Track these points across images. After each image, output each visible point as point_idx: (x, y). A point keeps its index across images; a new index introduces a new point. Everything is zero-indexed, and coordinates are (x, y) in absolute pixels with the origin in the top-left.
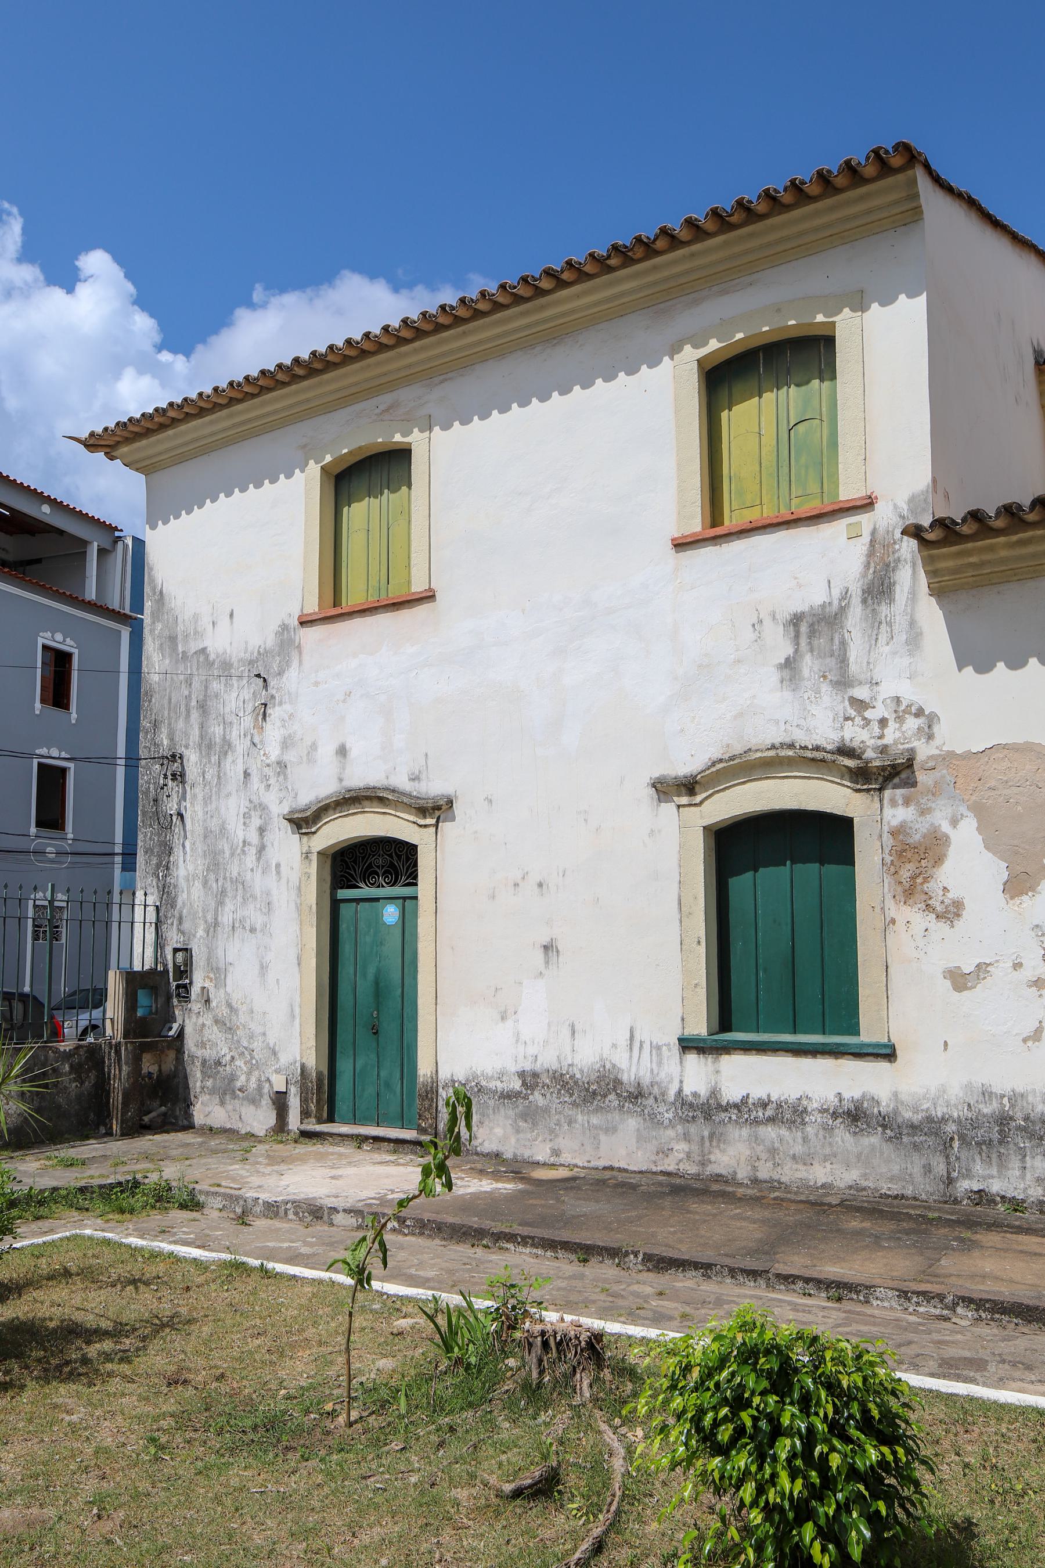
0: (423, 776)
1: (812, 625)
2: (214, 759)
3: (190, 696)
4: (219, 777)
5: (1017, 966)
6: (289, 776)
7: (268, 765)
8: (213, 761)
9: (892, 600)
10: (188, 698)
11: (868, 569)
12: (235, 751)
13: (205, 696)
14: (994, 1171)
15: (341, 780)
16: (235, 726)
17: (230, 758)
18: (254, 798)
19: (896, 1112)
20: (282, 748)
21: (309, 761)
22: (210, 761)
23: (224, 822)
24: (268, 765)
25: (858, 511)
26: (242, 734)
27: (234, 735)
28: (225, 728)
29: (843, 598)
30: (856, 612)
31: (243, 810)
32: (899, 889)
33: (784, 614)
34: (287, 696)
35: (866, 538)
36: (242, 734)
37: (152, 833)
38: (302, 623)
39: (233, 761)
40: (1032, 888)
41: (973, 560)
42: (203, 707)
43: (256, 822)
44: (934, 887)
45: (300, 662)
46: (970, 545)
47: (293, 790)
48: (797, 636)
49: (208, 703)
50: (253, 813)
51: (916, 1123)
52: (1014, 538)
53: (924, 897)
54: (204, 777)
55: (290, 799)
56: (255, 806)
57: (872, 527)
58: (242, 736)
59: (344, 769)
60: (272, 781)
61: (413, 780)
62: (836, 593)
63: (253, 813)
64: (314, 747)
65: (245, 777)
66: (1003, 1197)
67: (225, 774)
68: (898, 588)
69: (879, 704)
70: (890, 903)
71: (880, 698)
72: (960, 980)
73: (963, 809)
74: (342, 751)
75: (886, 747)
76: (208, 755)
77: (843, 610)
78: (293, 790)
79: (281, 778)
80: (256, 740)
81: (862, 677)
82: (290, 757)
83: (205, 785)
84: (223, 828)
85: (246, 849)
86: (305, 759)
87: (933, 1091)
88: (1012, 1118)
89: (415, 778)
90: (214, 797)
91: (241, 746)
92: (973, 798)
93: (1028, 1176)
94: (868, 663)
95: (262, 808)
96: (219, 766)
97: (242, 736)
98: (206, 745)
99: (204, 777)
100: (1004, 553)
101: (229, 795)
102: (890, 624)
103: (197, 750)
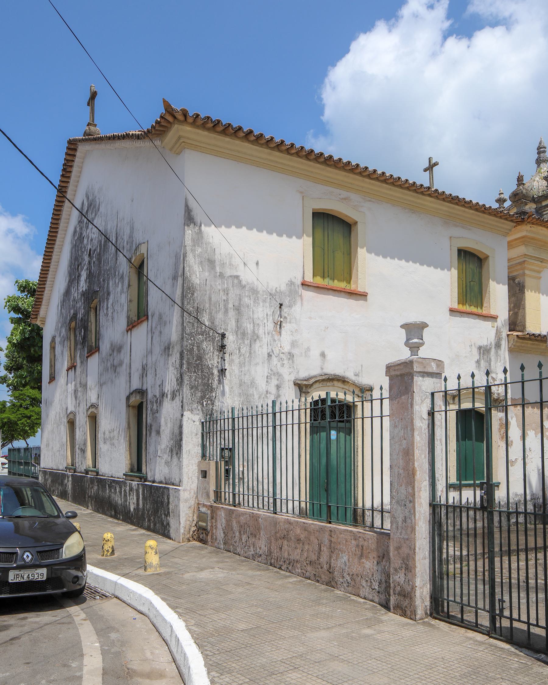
0: (360, 375)
1: (483, 351)
2: (247, 342)
3: (227, 300)
4: (250, 353)
6: (295, 361)
7: (283, 353)
8: (246, 343)
10: (226, 301)
12: (262, 341)
13: (239, 304)
15: (322, 369)
16: (261, 328)
17: (258, 344)
18: (274, 369)
20: (291, 346)
21: (306, 356)
22: (244, 343)
23: (253, 379)
24: (283, 353)
26: (266, 332)
27: (261, 332)
28: (254, 326)
29: (490, 345)
30: (493, 351)
31: (266, 374)
32: (501, 436)
33: (477, 345)
34: (294, 320)
35: (495, 328)
36: (266, 332)
37: (196, 377)
38: (302, 284)
39: (261, 346)
42: (238, 309)
43: (274, 382)
45: (302, 304)
47: (297, 369)
48: (480, 353)
49: (242, 309)
50: (273, 377)
54: (239, 351)
55: (295, 373)
56: (274, 374)
58: (266, 334)
59: (324, 364)
60: (285, 362)
61: (356, 375)
62: (489, 342)
63: (273, 377)
64: (308, 349)
65: (268, 357)
67: (254, 352)
68: (502, 346)
69: (498, 380)
70: (499, 440)
71: (498, 378)
73: (513, 415)
74: (323, 355)
75: (499, 393)
76: (243, 339)
77: (490, 348)
78: (297, 369)
79: (291, 361)
80: (276, 337)
82: (295, 351)
83: (240, 356)
84: (253, 383)
85: (268, 395)
86: (304, 354)
89: (356, 375)
90: (246, 363)
91: (266, 339)
95: (279, 375)
96: (251, 347)
97: (266, 334)
98: (241, 333)
99: (239, 351)
101: (257, 364)
102: (500, 356)
103: (234, 334)
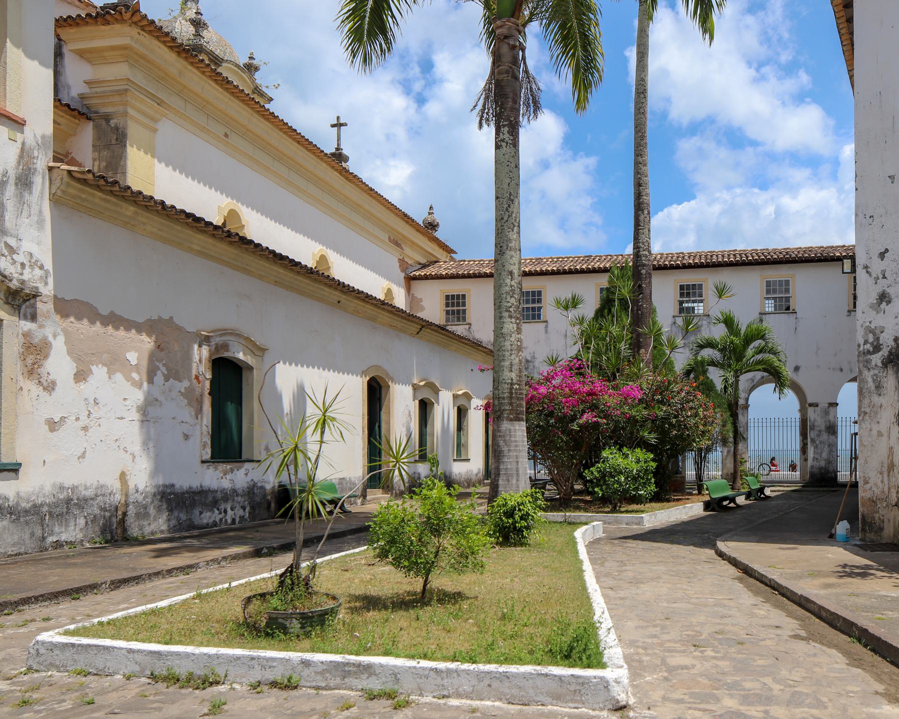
5: (77, 419)
9: (31, 193)
11: (20, 165)
14: (63, 529)
19: (18, 504)
25: (16, 125)
40: (85, 379)
41: (84, 196)
44: (42, 371)
46: (87, 189)
51: (28, 509)
52: (104, 196)
53: (39, 376)
57: (22, 140)
66: (66, 542)
72: (53, 425)
81: (13, 232)
87: (37, 489)
88: (72, 500)
92: (64, 325)
93: (77, 529)
94: (16, 225)
100: (97, 201)
